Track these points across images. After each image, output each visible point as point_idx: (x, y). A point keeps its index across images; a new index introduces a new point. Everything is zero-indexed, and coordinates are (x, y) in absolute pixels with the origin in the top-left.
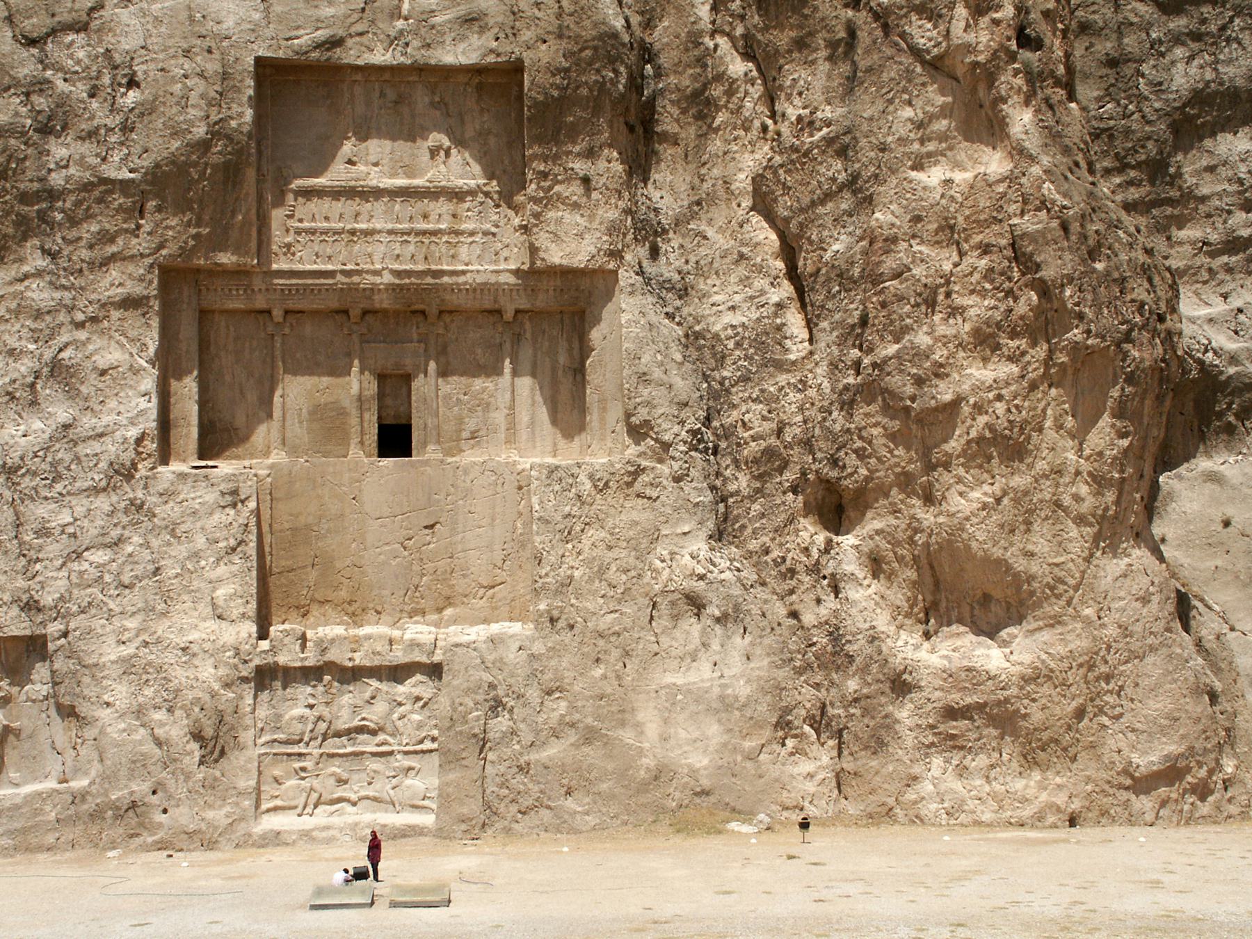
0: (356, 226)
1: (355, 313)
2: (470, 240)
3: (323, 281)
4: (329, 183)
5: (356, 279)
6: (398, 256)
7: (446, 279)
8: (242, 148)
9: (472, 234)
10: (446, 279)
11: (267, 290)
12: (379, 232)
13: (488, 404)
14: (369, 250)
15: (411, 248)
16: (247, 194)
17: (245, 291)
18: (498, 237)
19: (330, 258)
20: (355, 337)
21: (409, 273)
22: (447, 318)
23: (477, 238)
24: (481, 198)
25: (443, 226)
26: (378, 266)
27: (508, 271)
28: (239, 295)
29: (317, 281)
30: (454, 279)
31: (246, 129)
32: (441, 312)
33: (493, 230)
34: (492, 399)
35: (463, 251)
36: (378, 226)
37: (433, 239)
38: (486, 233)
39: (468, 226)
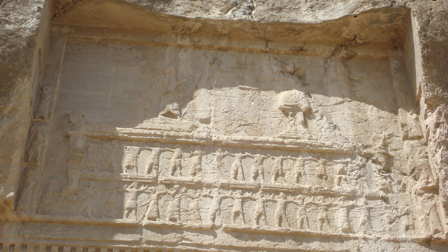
0: (173, 178)
2: (351, 203)
4: (140, 131)
5: (171, 237)
8: (17, 53)
9: (352, 196)
12: (209, 186)
16: (14, 110)
18: (393, 203)
23: (361, 202)
24: (359, 160)
26: (207, 223)
27: (413, 241)
31: (28, 33)
33: (382, 193)
36: (209, 179)
37: (290, 198)
38: (371, 197)
39: (347, 188)
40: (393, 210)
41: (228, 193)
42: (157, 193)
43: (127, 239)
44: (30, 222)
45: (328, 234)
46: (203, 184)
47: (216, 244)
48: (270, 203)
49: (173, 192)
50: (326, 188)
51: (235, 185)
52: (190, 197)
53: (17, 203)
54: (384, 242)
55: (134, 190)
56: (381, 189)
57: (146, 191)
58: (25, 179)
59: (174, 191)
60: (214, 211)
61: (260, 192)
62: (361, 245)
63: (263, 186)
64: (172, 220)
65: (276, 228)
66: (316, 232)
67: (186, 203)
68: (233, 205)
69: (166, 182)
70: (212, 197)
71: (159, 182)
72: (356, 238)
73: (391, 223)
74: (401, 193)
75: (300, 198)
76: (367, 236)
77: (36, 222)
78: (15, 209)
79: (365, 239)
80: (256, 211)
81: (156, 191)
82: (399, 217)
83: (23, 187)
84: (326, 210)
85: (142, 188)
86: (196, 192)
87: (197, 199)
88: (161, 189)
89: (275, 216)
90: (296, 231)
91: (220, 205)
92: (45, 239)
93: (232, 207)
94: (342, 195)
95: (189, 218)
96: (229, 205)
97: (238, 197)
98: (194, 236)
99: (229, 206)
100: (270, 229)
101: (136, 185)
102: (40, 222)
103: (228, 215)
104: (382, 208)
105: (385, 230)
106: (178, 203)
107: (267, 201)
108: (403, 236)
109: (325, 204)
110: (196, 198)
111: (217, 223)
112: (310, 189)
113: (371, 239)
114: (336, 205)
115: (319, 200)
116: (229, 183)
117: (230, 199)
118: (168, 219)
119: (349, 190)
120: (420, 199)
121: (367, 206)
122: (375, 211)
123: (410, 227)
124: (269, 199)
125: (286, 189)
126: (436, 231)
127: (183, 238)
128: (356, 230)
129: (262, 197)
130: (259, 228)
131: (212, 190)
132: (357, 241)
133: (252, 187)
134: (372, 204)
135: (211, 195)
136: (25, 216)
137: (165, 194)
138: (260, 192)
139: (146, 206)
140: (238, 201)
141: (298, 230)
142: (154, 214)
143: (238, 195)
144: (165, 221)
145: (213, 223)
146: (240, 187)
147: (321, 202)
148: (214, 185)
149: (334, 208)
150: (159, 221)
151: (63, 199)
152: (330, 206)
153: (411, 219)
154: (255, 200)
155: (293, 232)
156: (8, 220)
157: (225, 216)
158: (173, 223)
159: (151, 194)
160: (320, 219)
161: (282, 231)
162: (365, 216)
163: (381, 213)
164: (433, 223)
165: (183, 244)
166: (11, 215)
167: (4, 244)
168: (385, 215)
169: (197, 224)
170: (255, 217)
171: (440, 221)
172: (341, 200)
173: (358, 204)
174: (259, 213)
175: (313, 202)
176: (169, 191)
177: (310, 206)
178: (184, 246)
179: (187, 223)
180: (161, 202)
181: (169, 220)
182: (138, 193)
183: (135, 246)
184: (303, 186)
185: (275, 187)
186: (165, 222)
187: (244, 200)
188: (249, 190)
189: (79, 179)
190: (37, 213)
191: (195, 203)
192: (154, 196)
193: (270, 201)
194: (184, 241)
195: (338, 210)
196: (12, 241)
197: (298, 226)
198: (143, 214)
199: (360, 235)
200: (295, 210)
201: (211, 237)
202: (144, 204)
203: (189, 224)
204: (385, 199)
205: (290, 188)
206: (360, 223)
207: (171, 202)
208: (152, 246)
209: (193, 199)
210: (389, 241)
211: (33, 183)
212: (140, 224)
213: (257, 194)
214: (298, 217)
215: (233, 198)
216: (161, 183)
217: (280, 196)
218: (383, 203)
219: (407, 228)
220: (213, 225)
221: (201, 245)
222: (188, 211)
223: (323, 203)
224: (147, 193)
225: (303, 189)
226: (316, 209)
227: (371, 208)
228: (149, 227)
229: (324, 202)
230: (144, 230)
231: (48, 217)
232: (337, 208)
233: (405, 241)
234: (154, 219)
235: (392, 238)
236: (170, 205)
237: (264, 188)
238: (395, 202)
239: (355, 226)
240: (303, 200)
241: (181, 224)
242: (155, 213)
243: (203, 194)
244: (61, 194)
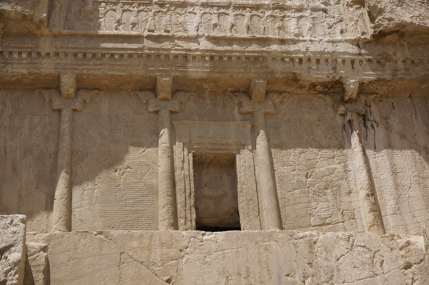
1: (165, 81)
2: (300, 14)
3: (126, 45)
5: (166, 45)
6: (215, 25)
7: (275, 47)
10: (275, 47)
11: (57, 54)
13: (339, 187)
14: (181, 19)
15: (230, 19)
17: (30, 54)
18: (330, 13)
19: (134, 25)
20: (165, 114)
21: (230, 41)
22: (276, 98)
23: (307, 13)
25: (267, 3)
26: (192, 33)
27: (346, 41)
28: (23, 59)
29: (119, 46)
30: (284, 47)
32: (267, 93)
33: (323, 6)
34: (344, 183)
35: (292, 26)
37: (254, 12)
38: (314, 10)
40: (331, 18)
41: (207, 10)
42: (153, 11)
43: (133, 47)
44: (59, 36)
45: (284, 38)
46: (188, 3)
47: (200, 49)
48: (240, 16)
49: (165, 10)
50: (281, 4)
51: (212, 3)
52: (178, 14)
53: (48, 21)
54: (325, 42)
55: (135, 9)
56: (322, 3)
57: (144, 10)
58: (52, 3)
59: (166, 10)
60: (198, 24)
61: (232, 8)
62: (309, 45)
63: (234, 3)
64: (166, 31)
65: (245, 36)
66: (275, 37)
67: (176, 18)
68: (212, 19)
69: (160, 2)
70: (195, 14)
71: (154, 3)
72: (304, 41)
73: (330, 28)
74: (337, 6)
75: (261, 12)
76: (312, 39)
77: (64, 35)
78: (48, 26)
79: (311, 41)
80: (229, 23)
81: (152, 9)
82: (336, 24)
83: (52, 9)
84: (282, 20)
85: (142, 8)
86: (183, 10)
87: (184, 15)
88: (155, 8)
89: (244, 26)
90: (260, 37)
91: (201, 19)
92: (72, 48)
93: (211, 20)
94: (293, 9)
95: (179, 30)
96: (208, 19)
97: (215, 13)
98: (184, 43)
99: (208, 20)
100: (241, 36)
101: (136, 6)
102: (67, 35)
103: (208, 26)
104: (323, 17)
105: (325, 34)
106: (169, 18)
107: (237, 15)
108: (339, 37)
109: (281, 15)
110: (183, 14)
111: (200, 33)
112: (269, 5)
113: (316, 41)
114: (289, 17)
115: (276, 13)
116: (208, 2)
117: (209, 15)
118: (163, 31)
119: (298, 4)
120: (351, 9)
121: (312, 16)
122: (318, 20)
123: (344, 31)
124: (238, 13)
125: (251, 5)
126: (363, 33)
127: (176, 45)
128: (304, 34)
129: (233, 12)
130: (232, 35)
131: (195, 8)
132: (306, 42)
133: (225, 5)
134: (315, 14)
135: (195, 11)
136: (55, 31)
137: (159, 12)
138: (232, 8)
139: (146, 21)
140: (215, 16)
141: (262, 36)
142: (152, 28)
143: (215, 11)
144: (161, 33)
145: (197, 33)
146: (216, 4)
147: (278, 14)
148: (196, 3)
149: (288, 19)
150: (157, 32)
151: (83, 17)
152: (284, 17)
153: (344, 25)
154: (228, 14)
155: (258, 38)
156: (43, 34)
157: (206, 28)
158: (167, 34)
159: (148, 12)
160: (277, 28)
161: (250, 37)
162: (310, 24)
163: (322, 21)
164: (361, 27)
165: (175, 50)
166: (45, 31)
167: (41, 53)
168: (326, 23)
169: (185, 35)
170: (229, 27)
171: (366, 26)
172: (292, 12)
173: (306, 15)
174: (232, 24)
175: (272, 14)
176: (162, 10)
177: (270, 18)
178: (177, 51)
179: (177, 33)
180: (157, 18)
181: (164, 31)
182: (139, 11)
183: (140, 52)
184: (264, 3)
185: (243, 4)
186: (161, 34)
187: (219, 15)
188: (224, 7)
189: (93, 1)
190: (64, 29)
191: (183, 18)
192: (151, 14)
193: (239, 15)
194: (176, 48)
195: (291, 20)
196: (48, 50)
197: (262, 33)
198: (144, 28)
199: (307, 38)
200: (258, 21)
201: (196, 44)
202: (144, 20)
203: (179, 34)
204: (325, 11)
205: (254, 4)
206: (307, 29)
207: (164, 18)
208: (153, 52)
209: (181, 15)
210: (328, 42)
211: (59, 6)
212: (142, 35)
213: (229, 10)
214: (261, 26)
215: (211, 14)
216: (156, 3)
217: (247, 11)
218: (324, 13)
219: (342, 32)
220: (198, 34)
221: (189, 50)
222: (177, 24)
223: (279, 15)
224: (145, 11)
225: (264, 4)
226: (274, 20)
227: (315, 18)
228: (149, 37)
229: (280, 14)
230: (145, 40)
231: (73, 32)
232: (290, 18)
233: (340, 41)
234: (153, 31)
235: (331, 39)
236: (163, 20)
237: (235, 5)
238: (332, 13)
239: (303, 32)
240: (264, 13)
241: (173, 34)
242: (153, 27)
243: (188, 11)
244: (80, 14)
